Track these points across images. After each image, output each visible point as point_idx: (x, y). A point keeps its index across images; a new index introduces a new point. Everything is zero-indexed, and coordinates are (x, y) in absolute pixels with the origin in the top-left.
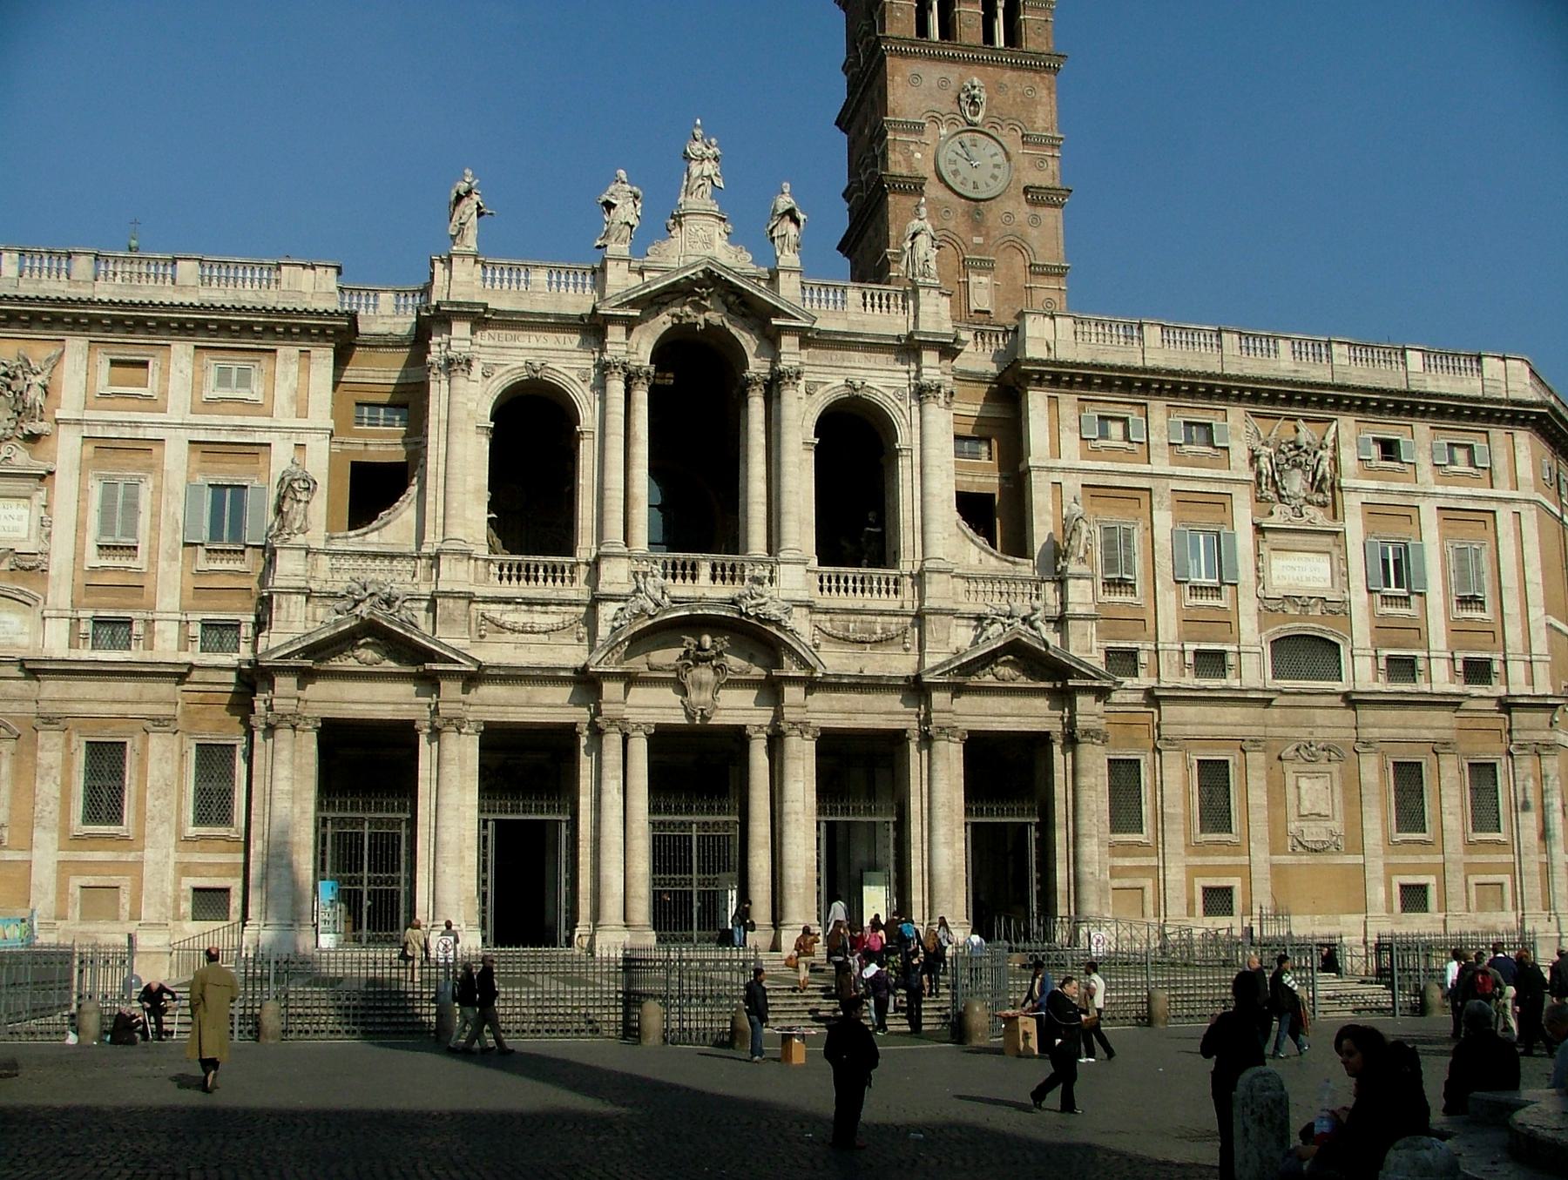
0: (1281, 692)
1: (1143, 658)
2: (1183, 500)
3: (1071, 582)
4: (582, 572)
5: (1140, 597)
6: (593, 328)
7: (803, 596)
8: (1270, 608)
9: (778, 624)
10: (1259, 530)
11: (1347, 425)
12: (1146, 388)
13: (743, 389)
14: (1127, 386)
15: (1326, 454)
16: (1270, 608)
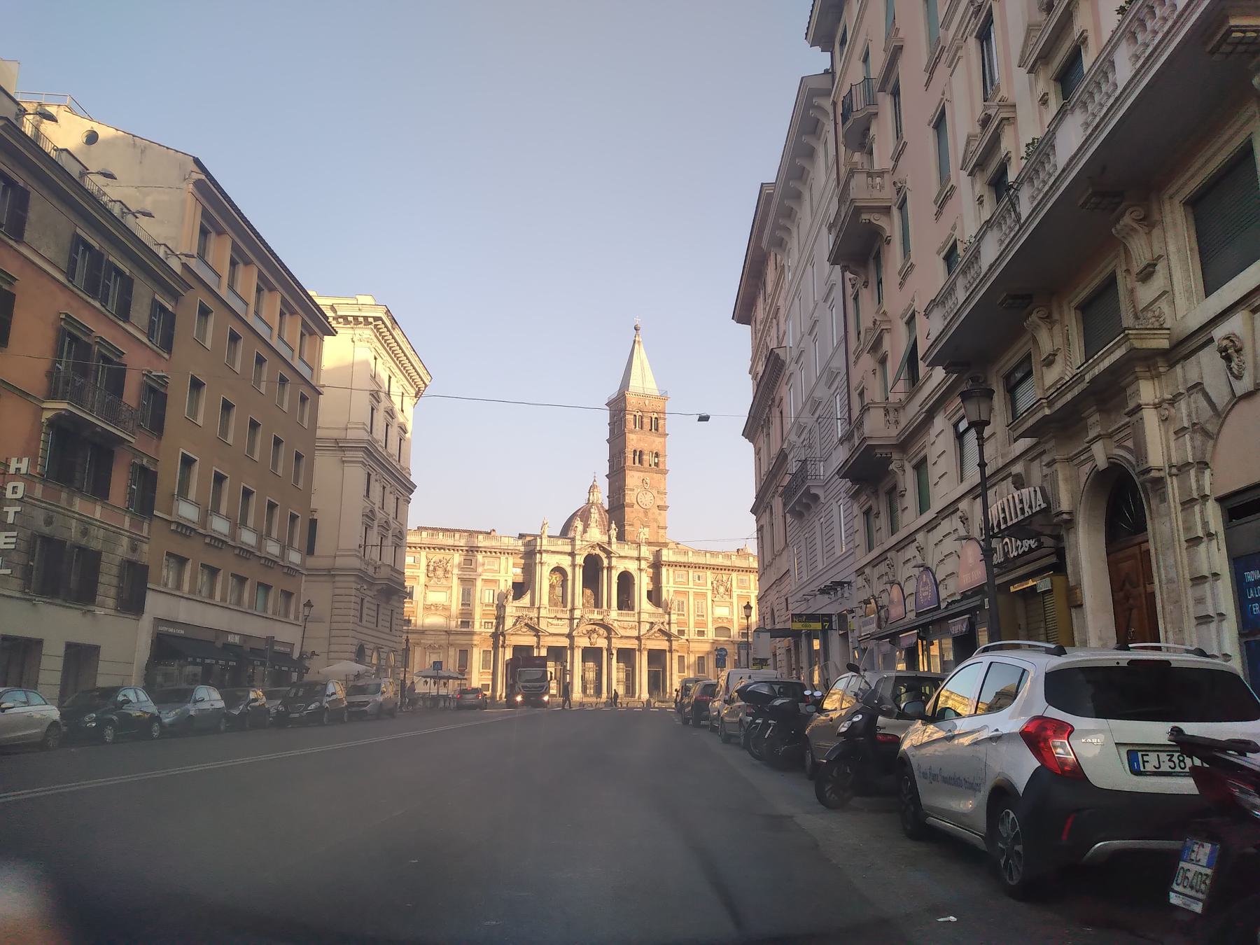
0: (717, 640)
1: (686, 631)
2: (696, 594)
3: (672, 615)
4: (568, 612)
5: (686, 617)
6: (572, 554)
7: (616, 618)
8: (715, 620)
9: (612, 625)
10: (713, 600)
11: (734, 575)
12: (689, 567)
13: (602, 569)
14: (685, 566)
15: (729, 583)
16: (715, 620)
